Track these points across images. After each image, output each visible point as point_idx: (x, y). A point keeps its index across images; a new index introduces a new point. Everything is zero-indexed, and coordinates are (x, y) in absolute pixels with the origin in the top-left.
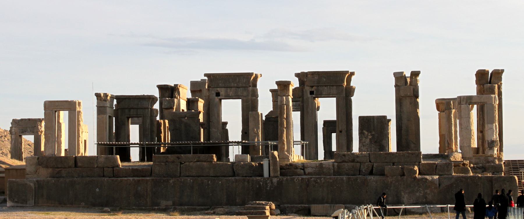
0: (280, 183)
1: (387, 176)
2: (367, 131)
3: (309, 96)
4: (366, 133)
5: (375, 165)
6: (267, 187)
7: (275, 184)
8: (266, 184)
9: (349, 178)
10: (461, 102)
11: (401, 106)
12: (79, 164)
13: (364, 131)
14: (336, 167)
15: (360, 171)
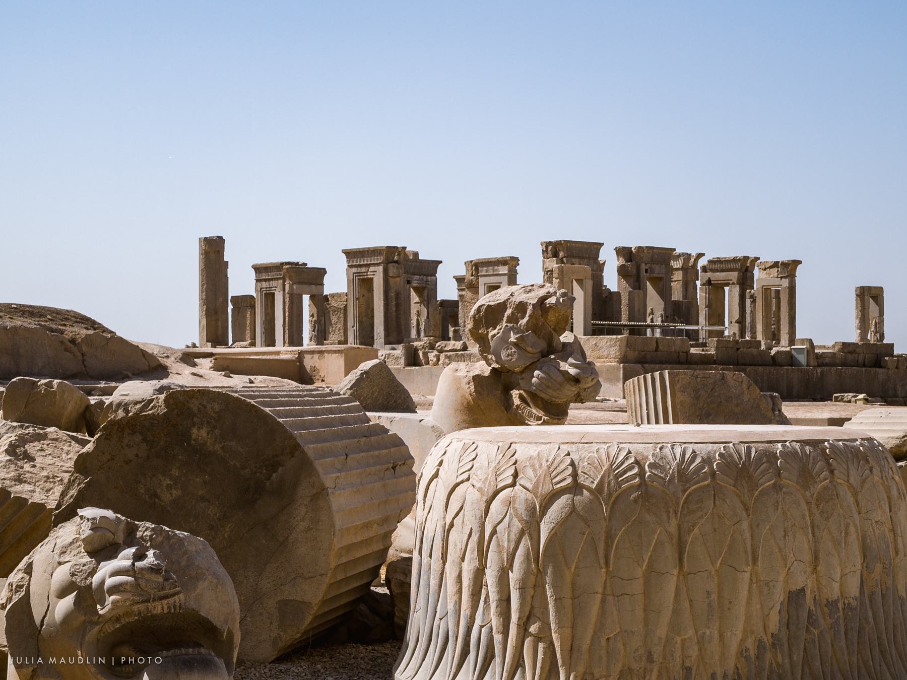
0: (822, 372)
1: (888, 369)
2: (678, 317)
3: (645, 274)
4: (677, 319)
5: (867, 356)
6: (813, 378)
7: (819, 375)
8: (813, 374)
9: (866, 371)
10: (864, 292)
11: (686, 290)
12: (661, 347)
13: (676, 317)
14: (843, 357)
15: (858, 361)
